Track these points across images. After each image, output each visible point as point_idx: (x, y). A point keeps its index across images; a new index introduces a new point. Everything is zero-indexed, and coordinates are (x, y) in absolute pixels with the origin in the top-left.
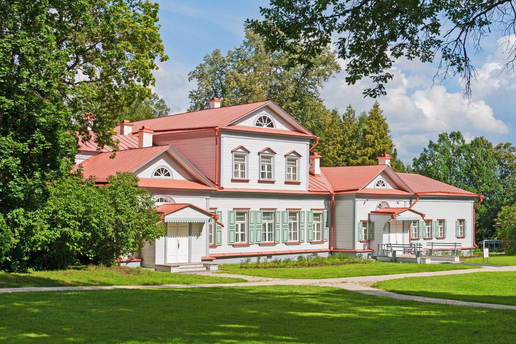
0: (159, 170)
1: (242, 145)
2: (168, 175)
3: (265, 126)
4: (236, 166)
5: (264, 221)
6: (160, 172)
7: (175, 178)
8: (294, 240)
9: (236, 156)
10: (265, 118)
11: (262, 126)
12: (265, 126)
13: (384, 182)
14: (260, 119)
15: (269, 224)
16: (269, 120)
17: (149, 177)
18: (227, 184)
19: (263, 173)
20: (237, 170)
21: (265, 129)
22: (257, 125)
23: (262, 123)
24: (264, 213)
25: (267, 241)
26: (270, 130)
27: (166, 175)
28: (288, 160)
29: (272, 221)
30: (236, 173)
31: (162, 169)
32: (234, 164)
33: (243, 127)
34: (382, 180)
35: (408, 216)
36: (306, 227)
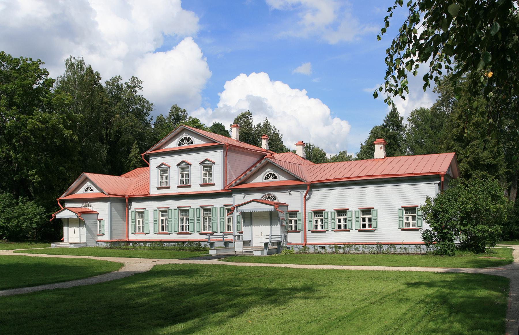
0: (87, 188)
2: (92, 190)
3: (186, 145)
4: (162, 178)
5: (182, 217)
7: (95, 192)
9: (162, 171)
10: (185, 138)
11: (183, 145)
12: (186, 145)
13: (276, 175)
14: (182, 140)
15: (186, 218)
16: (189, 139)
17: (82, 193)
18: (154, 192)
20: (162, 181)
21: (188, 146)
22: (179, 145)
23: (183, 143)
24: (181, 210)
25: (185, 231)
26: (191, 146)
28: (204, 167)
29: (188, 217)
30: (161, 183)
31: (89, 187)
33: (170, 148)
34: (272, 173)
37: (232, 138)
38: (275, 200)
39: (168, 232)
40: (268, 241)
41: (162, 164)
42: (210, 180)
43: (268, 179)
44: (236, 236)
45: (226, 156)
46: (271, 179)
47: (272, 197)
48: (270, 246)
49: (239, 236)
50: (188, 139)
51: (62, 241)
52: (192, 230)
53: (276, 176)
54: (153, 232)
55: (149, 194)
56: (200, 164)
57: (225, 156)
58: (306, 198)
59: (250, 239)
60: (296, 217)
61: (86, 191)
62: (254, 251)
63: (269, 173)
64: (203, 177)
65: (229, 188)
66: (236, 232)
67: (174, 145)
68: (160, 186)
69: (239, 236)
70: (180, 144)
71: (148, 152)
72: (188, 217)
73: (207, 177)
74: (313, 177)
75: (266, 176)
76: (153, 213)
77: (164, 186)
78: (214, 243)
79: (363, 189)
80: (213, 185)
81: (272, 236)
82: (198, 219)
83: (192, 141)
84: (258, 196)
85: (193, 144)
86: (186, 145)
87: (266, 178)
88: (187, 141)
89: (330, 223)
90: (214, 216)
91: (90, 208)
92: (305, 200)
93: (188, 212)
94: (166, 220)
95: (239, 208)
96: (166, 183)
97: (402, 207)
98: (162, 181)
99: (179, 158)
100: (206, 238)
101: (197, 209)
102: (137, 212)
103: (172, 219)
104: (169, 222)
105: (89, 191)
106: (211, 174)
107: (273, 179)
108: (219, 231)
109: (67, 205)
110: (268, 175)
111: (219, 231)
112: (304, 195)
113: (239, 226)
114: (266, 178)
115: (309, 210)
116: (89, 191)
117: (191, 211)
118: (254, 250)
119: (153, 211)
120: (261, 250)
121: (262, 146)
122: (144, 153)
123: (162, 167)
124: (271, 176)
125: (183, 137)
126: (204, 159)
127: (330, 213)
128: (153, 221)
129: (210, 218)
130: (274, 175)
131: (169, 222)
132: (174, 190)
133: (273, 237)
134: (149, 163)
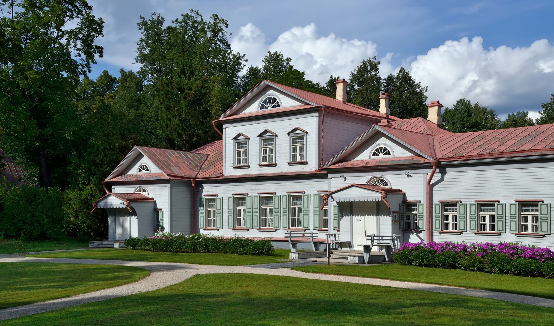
0: (141, 167)
1: (240, 132)
3: (270, 108)
6: (142, 169)
8: (298, 226)
9: (239, 144)
10: (270, 99)
11: (267, 108)
12: (270, 108)
14: (265, 102)
15: (270, 209)
16: (275, 100)
18: (229, 171)
19: (295, 155)
20: (239, 158)
27: (146, 171)
29: (271, 206)
31: (144, 166)
32: (263, 149)
35: (349, 196)
36: (312, 211)
37: (337, 98)
38: (387, 185)
39: (245, 227)
40: (369, 243)
41: (239, 135)
42: (302, 156)
43: (377, 155)
44: (332, 235)
45: (323, 124)
46: (381, 156)
47: (382, 181)
48: (375, 250)
49: (335, 235)
50: (273, 101)
51: (107, 239)
52: (276, 225)
53: (388, 151)
54: (227, 227)
55: (223, 176)
56: (288, 134)
57: (321, 123)
58: (431, 183)
59: (349, 240)
60: (416, 211)
61: (140, 170)
62: (349, 257)
63: (378, 147)
64: (292, 153)
65: (324, 168)
66: (332, 229)
67: (253, 109)
68: (236, 165)
69: (335, 235)
70: (262, 107)
71: (221, 118)
72: (271, 206)
73: (298, 153)
74: (445, 153)
75: (374, 151)
76: (227, 201)
77: (242, 164)
78: (297, 243)
79: (528, 170)
80: (306, 163)
81: (374, 236)
82: (284, 210)
83: (278, 102)
84: (363, 178)
85: (279, 106)
86: (270, 109)
87: (375, 154)
88: (272, 104)
89: (468, 220)
90: (306, 206)
91: (145, 194)
92: (431, 187)
93: (273, 201)
94: (244, 210)
95: (333, 195)
96: (245, 160)
97: (440, 202)
98: (239, 158)
99: (261, 126)
100: (286, 237)
101: (283, 196)
102: (207, 199)
103: (251, 210)
104: (218, 215)
105: (144, 171)
106: (302, 149)
107: (384, 155)
108: (312, 228)
109: (117, 189)
110: (377, 150)
111: (312, 228)
112: (428, 178)
113: (336, 221)
114: (375, 154)
115: (436, 201)
116: (144, 171)
117: (276, 199)
118: (349, 256)
119: (227, 198)
120: (358, 256)
121: (380, 110)
122: (216, 120)
123: (238, 138)
124: (383, 152)
125: (267, 97)
126: (293, 128)
127: (468, 206)
128: (227, 212)
129: (300, 209)
130: (387, 149)
131: (218, 215)
132: (255, 170)
133: (375, 238)
134: (222, 134)
